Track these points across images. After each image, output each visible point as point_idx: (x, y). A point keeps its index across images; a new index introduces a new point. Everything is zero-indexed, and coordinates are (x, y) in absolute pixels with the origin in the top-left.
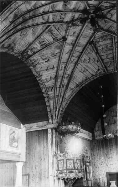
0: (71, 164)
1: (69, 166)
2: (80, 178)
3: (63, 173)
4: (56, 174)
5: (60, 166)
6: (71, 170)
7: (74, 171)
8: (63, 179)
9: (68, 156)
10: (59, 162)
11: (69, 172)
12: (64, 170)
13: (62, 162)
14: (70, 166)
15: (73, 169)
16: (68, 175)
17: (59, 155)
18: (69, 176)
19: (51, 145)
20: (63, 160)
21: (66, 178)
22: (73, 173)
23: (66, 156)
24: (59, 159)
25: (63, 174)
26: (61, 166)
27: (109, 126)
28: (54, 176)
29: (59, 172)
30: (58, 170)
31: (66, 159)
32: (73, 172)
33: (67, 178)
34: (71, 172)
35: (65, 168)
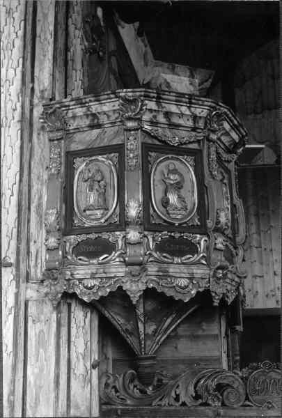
0: (178, 186)
1: (165, 203)
3: (109, 248)
4: (39, 262)
5: (86, 197)
6: (182, 228)
7: (202, 242)
8: (91, 306)
9: (161, 119)
10: (81, 165)
11: (159, 248)
12: (124, 224)
13: (106, 163)
14: (173, 198)
15: (193, 229)
16: (152, 269)
17: (80, 111)
18: (164, 275)
19: (18, 43)
20: (120, 149)
21: (134, 289)
22: (195, 258)
23: (147, 117)
24: (74, 147)
25: (115, 254)
26: (92, 198)
27: (259, 116)
28: (28, 279)
29: (72, 239)
30: (68, 224)
31: (146, 148)
32: (193, 249)
33: (149, 294)
34: (177, 246)
35: (133, 211)
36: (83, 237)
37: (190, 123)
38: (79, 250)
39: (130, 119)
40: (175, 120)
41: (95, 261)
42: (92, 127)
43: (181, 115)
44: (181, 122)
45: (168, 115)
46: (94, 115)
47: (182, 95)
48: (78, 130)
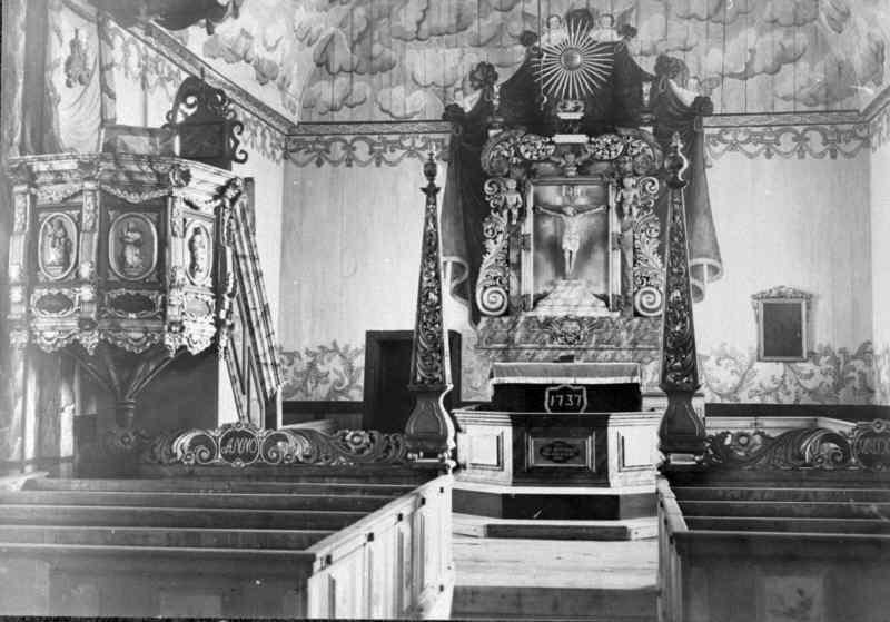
1: (122, 260)
2: (195, 350)
17: (43, 167)
22: (150, 314)
35: (86, 271)
36: (45, 292)
37: (154, 179)
38: (44, 304)
39: (88, 179)
40: (138, 178)
41: (54, 315)
42: (56, 182)
43: (143, 173)
44: (144, 179)
45: (129, 174)
46: (58, 173)
47: (142, 156)
48: (44, 183)
